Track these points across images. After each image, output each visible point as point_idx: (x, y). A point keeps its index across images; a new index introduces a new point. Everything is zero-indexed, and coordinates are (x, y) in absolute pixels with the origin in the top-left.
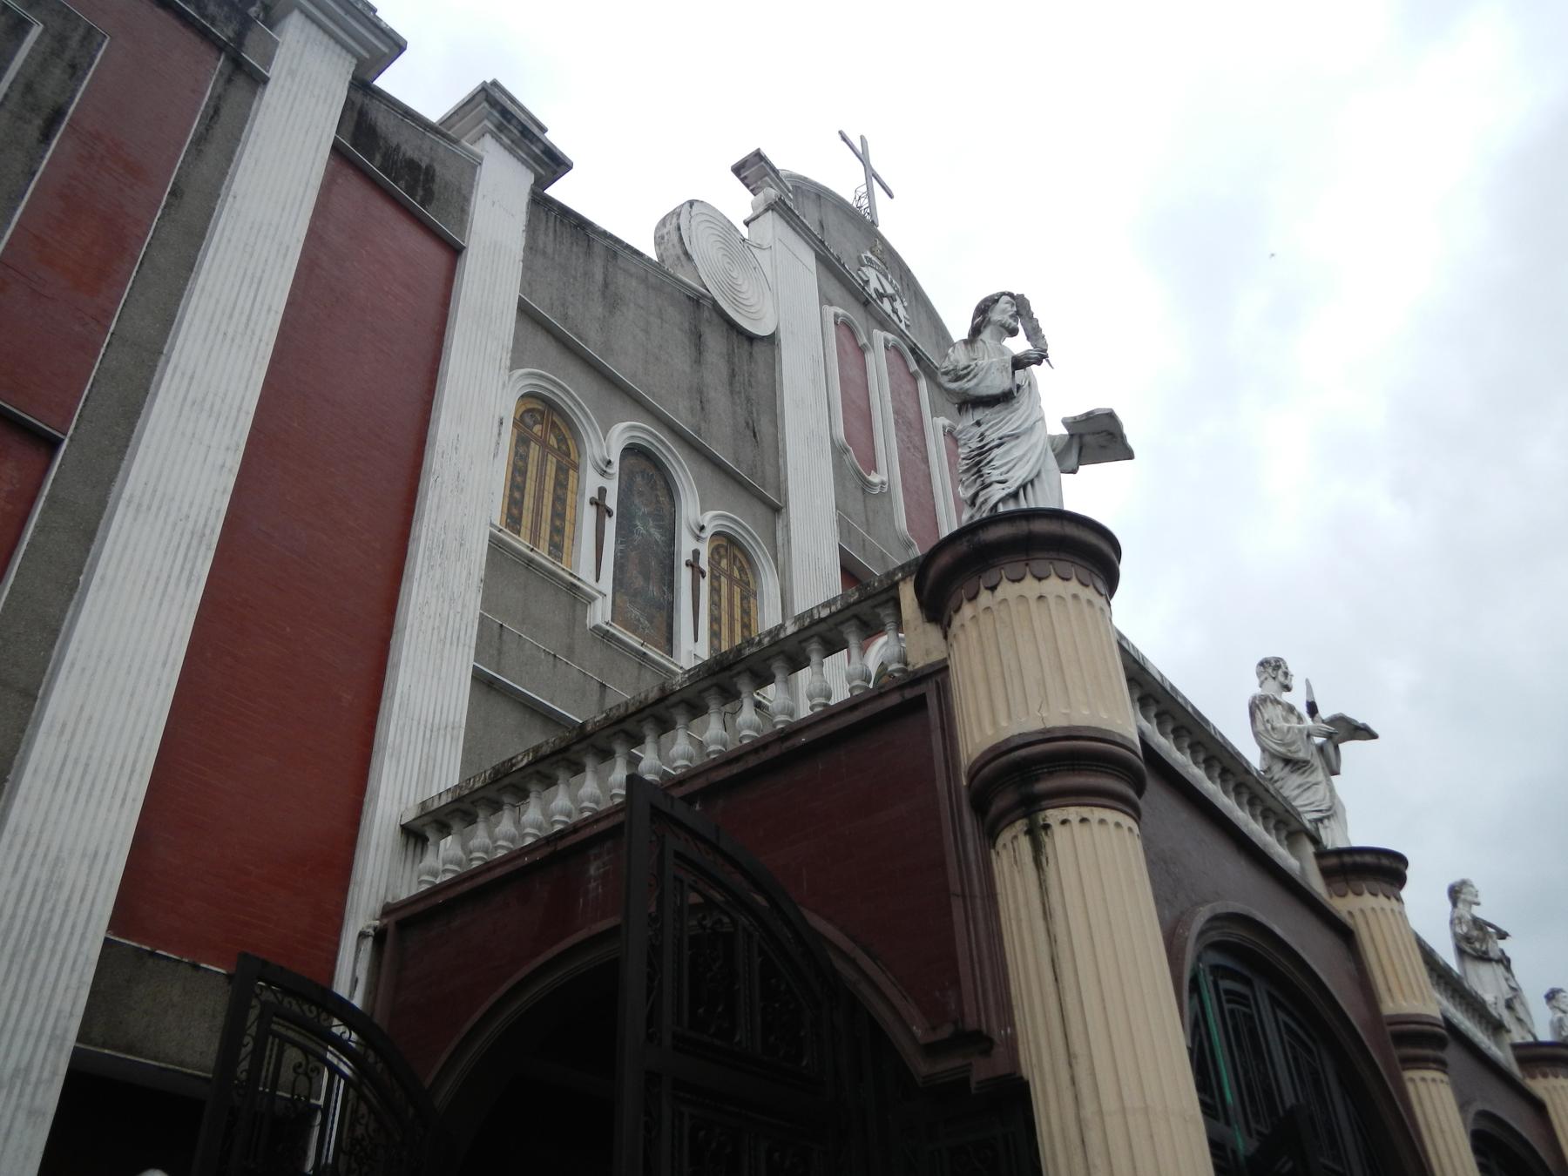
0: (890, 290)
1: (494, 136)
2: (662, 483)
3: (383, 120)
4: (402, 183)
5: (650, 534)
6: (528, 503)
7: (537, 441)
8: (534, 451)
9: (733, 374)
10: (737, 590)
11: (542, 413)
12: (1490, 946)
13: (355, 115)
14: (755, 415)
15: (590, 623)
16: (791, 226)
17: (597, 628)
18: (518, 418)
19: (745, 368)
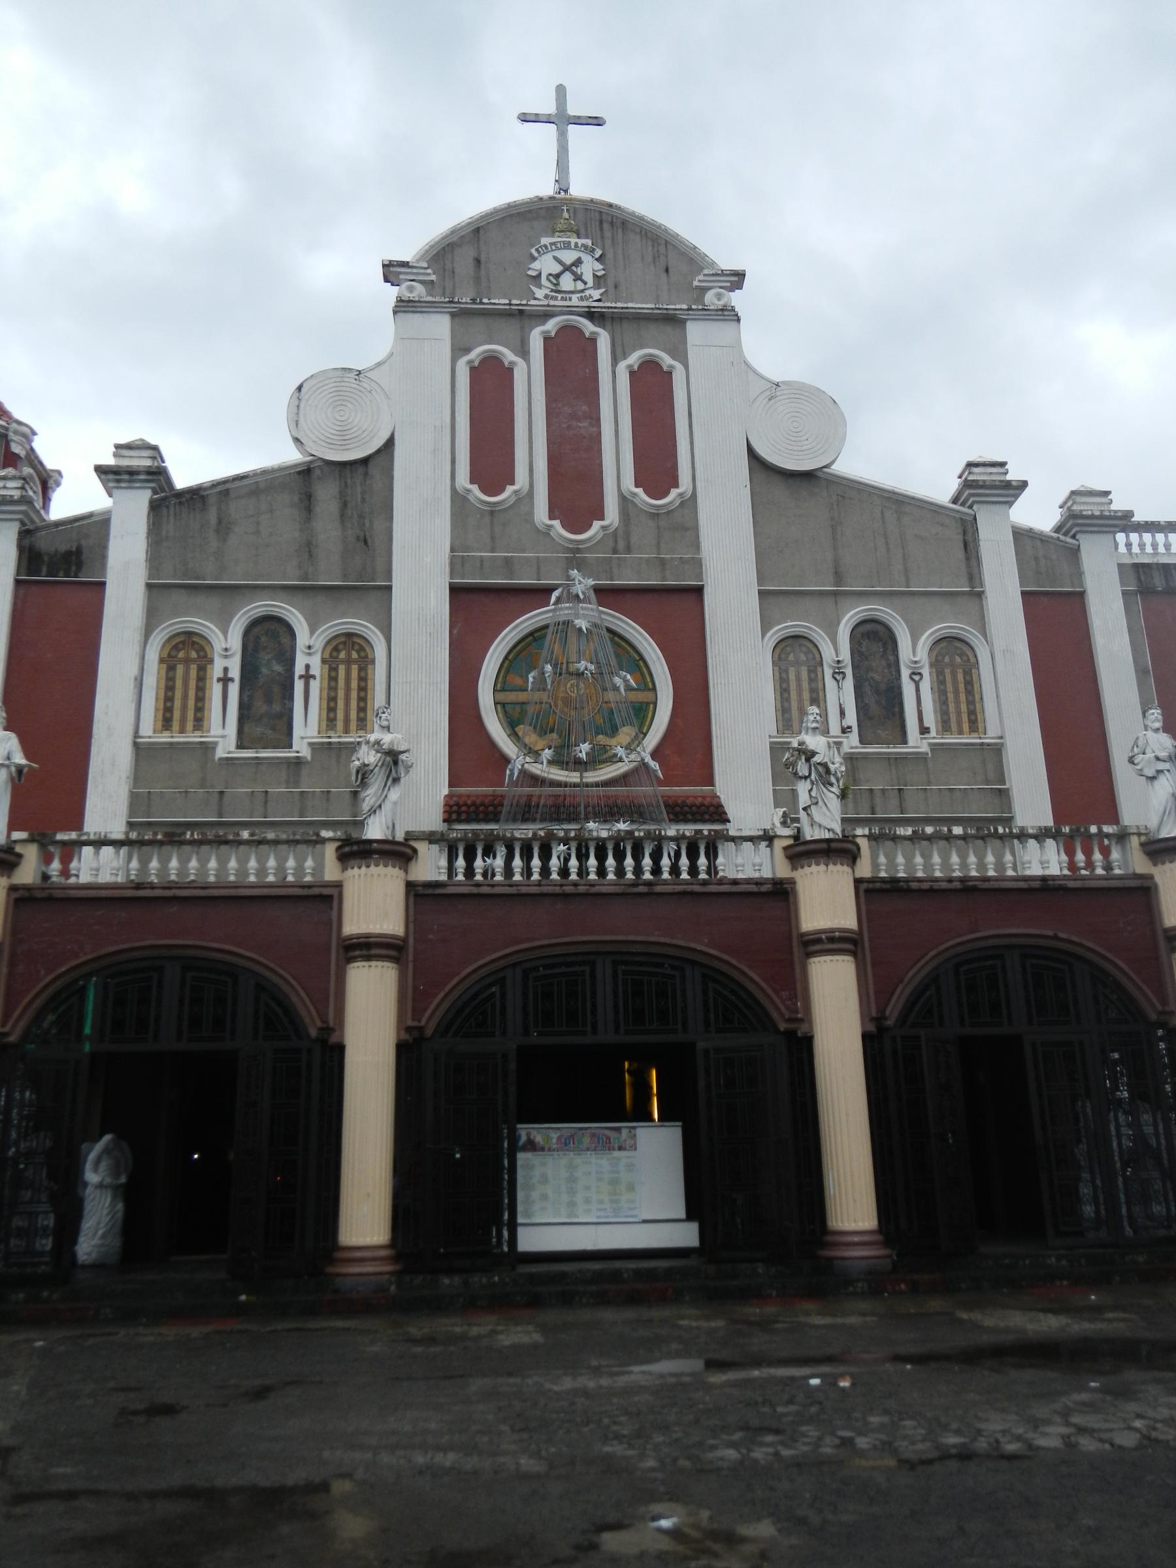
0: (569, 257)
1: (117, 488)
2: (285, 629)
3: (43, 543)
4: (61, 573)
5: (273, 671)
6: (177, 704)
7: (180, 661)
8: (180, 669)
9: (345, 505)
10: (355, 668)
11: (183, 642)
12: (799, 767)
13: (27, 554)
14: (367, 525)
15: (217, 757)
16: (417, 312)
17: (220, 759)
18: (166, 656)
19: (359, 490)
